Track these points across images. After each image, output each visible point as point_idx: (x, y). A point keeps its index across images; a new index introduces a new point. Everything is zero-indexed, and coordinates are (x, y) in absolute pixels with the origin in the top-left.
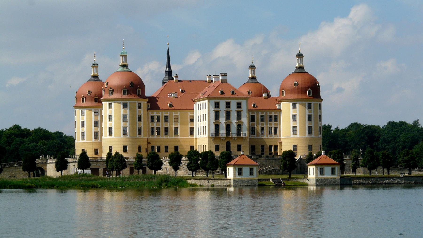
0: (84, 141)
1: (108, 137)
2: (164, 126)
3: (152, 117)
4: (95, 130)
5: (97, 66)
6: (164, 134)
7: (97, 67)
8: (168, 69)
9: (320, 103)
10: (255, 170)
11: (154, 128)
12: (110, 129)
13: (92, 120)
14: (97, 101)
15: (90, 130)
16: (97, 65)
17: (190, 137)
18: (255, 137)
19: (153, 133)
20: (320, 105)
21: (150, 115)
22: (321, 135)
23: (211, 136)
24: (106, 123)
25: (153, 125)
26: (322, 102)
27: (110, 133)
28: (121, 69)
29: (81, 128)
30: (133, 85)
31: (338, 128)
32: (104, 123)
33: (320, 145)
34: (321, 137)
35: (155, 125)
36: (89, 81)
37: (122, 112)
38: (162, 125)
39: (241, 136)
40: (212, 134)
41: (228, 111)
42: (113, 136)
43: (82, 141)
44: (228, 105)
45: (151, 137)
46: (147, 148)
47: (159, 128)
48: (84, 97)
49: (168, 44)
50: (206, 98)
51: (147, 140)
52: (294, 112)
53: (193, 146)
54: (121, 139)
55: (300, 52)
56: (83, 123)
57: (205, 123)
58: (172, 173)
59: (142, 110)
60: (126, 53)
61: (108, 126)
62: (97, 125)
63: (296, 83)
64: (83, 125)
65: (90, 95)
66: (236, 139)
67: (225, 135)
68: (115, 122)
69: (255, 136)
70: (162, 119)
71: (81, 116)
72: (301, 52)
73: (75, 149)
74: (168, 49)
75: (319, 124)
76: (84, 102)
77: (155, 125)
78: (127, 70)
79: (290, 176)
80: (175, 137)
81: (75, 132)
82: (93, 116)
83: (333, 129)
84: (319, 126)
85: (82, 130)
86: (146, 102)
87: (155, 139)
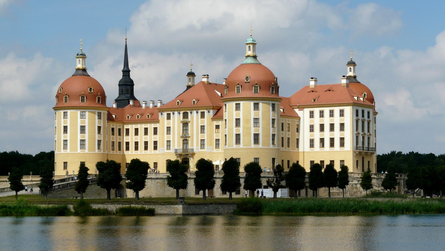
4: (81, 138)
5: (85, 56)
7: (85, 58)
12: (238, 136)
13: (95, 125)
14: (99, 102)
15: (92, 137)
16: (85, 55)
23: (354, 150)
28: (250, 61)
32: (243, 128)
36: (72, 76)
37: (271, 115)
42: (260, 146)
48: (83, 94)
49: (126, 39)
54: (270, 149)
58: (353, 193)
60: (255, 41)
63: (365, 94)
65: (92, 93)
68: (263, 128)
72: (353, 60)
73: (55, 162)
81: (55, 140)
82: (97, 120)
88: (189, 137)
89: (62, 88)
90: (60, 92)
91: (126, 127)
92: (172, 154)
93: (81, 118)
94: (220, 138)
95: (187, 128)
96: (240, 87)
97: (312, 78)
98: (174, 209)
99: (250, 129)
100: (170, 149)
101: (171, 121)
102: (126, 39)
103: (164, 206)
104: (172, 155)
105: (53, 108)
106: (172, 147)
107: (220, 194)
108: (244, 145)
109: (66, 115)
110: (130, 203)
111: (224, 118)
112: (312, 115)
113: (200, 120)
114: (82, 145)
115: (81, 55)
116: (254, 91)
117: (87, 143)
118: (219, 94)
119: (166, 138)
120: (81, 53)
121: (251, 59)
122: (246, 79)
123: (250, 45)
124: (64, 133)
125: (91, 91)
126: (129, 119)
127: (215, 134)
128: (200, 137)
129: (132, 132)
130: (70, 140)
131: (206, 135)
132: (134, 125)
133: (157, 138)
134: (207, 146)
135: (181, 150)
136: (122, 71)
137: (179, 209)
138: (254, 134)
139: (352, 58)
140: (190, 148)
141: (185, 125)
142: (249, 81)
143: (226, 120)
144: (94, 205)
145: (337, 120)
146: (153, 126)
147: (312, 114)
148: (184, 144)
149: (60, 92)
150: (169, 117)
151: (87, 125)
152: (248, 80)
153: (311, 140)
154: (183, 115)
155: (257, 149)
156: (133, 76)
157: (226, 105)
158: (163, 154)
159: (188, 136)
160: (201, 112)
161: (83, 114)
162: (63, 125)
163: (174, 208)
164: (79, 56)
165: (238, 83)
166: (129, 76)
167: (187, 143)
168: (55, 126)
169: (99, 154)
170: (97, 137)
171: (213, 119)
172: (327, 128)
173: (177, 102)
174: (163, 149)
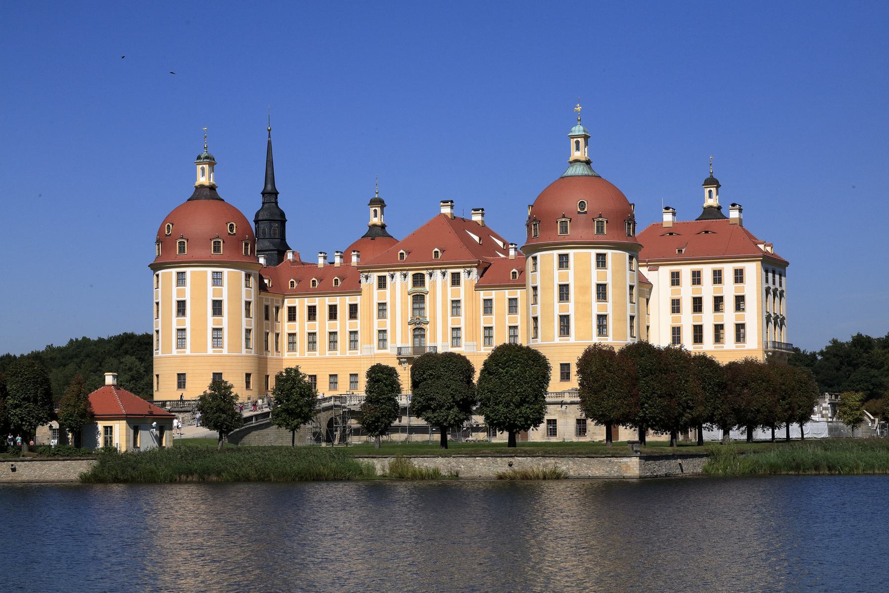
16: (214, 160)
32: (576, 303)
56: (181, 305)
62: (220, 313)
71: (174, 288)
88: (427, 323)
89: (173, 225)
90: (169, 232)
91: (288, 303)
92: (390, 356)
94: (518, 324)
95: (422, 306)
96: (569, 222)
97: (667, 208)
98: (620, 466)
99: (590, 305)
100: (384, 347)
101: (388, 291)
102: (269, 131)
103: (595, 460)
104: (365, 359)
105: (149, 266)
106: (389, 343)
107: (543, 436)
108: (577, 338)
109: (182, 279)
110: (514, 455)
111: (530, 284)
112: (675, 279)
113: (450, 288)
114: (216, 340)
115: (207, 158)
116: (597, 231)
117: (225, 334)
118: (476, 238)
119: (376, 325)
120: (204, 154)
121: (582, 167)
122: (579, 207)
123: (579, 139)
124: (178, 315)
125: (232, 230)
126: (295, 288)
127: (482, 317)
128: (451, 323)
129: (302, 313)
130: (192, 330)
131: (462, 318)
132: (306, 299)
133: (357, 324)
134: (466, 341)
135: (410, 350)
136: (262, 193)
137: (631, 466)
138: (598, 315)
139: (712, 173)
140: (428, 346)
141: (419, 299)
142: (586, 210)
143: (535, 288)
144: (426, 459)
145: (729, 289)
146: (348, 300)
147: (675, 279)
148: (415, 336)
149: (169, 232)
150: (382, 283)
151: (225, 298)
152: (584, 209)
153: (674, 328)
154: (414, 279)
156: (283, 203)
157: (535, 258)
158: (370, 357)
159: (426, 321)
160: (453, 274)
161: (217, 276)
162: (175, 299)
163: (619, 464)
164: (202, 161)
165: (600, 214)
166: (276, 203)
167: (423, 336)
168: (155, 301)
169: (247, 358)
170: (244, 323)
171: (478, 287)
172: (708, 304)
173: (399, 253)
174: (371, 348)
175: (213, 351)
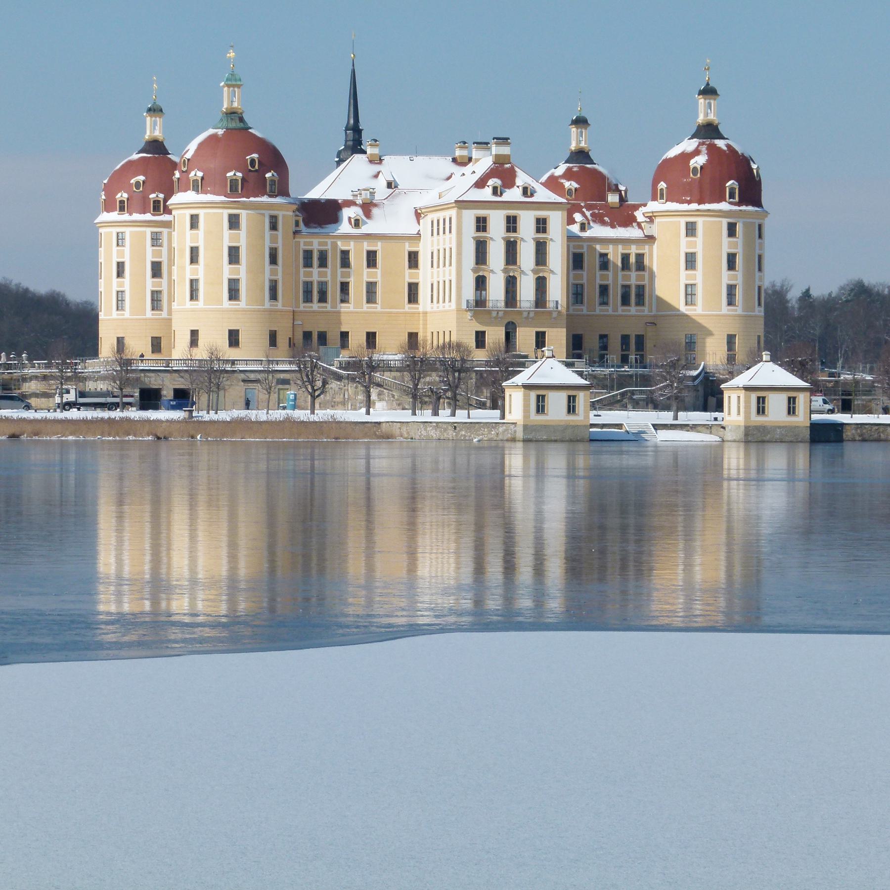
0: (123, 315)
1: (189, 304)
2: (340, 279)
3: (308, 255)
6: (338, 300)
8: (352, 121)
9: (760, 221)
10: (582, 399)
11: (311, 283)
12: (194, 284)
16: (161, 110)
17: (408, 307)
18: (585, 312)
19: (308, 298)
20: (760, 226)
21: (303, 247)
22: (762, 309)
23: (464, 306)
24: (183, 268)
25: (310, 274)
26: (766, 219)
27: (194, 295)
29: (115, 280)
30: (257, 167)
31: (808, 290)
33: (759, 337)
34: (762, 314)
35: (315, 274)
38: (332, 275)
39: (546, 308)
40: (468, 301)
41: (512, 240)
42: (200, 304)
43: (118, 315)
44: (512, 223)
45: (304, 307)
46: (291, 337)
47: (326, 283)
50: (454, 205)
51: (293, 315)
52: (689, 244)
53: (416, 334)
55: (708, 84)
56: (120, 267)
57: (449, 273)
59: (280, 233)
61: (188, 277)
64: (120, 273)
66: (532, 315)
67: (503, 304)
69: (584, 308)
70: (334, 260)
71: (115, 248)
72: (712, 84)
73: (100, 336)
74: (353, 72)
75: (757, 280)
76: (124, 211)
77: (315, 274)
78: (242, 125)
79: (676, 418)
80: (368, 308)
83: (794, 295)
84: (757, 283)
85: (117, 287)
86: (291, 213)
87: (314, 312)
93: (153, 246)
151: (127, 260)
155: (193, 311)
175: (152, 314)
